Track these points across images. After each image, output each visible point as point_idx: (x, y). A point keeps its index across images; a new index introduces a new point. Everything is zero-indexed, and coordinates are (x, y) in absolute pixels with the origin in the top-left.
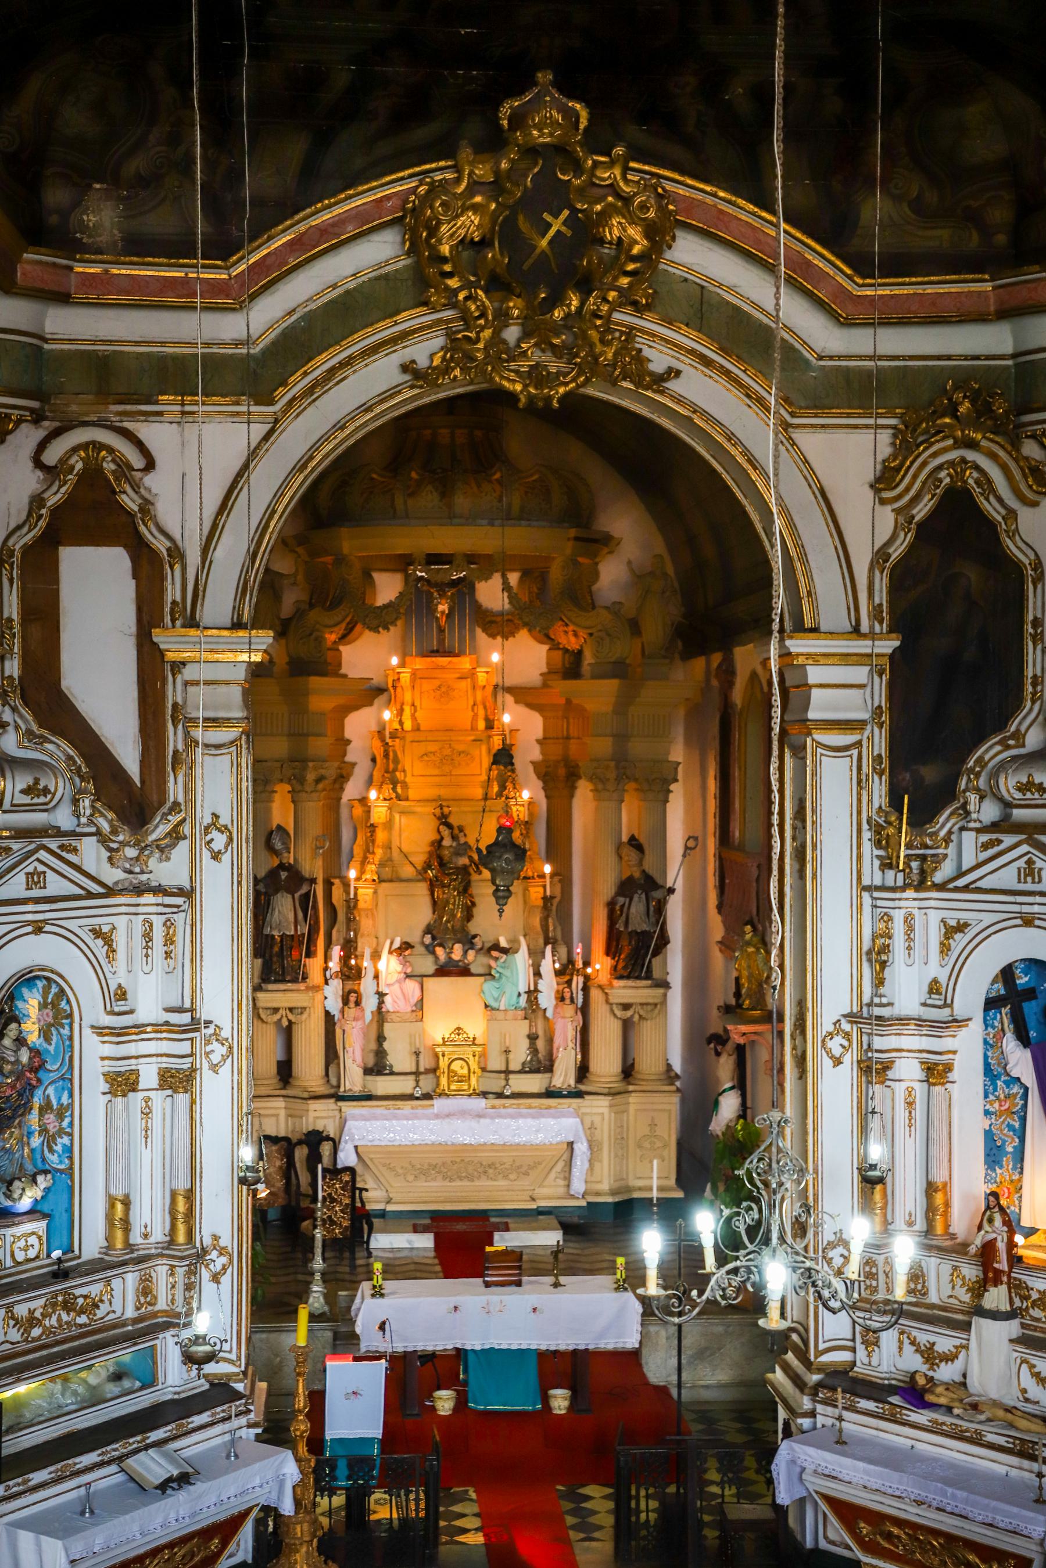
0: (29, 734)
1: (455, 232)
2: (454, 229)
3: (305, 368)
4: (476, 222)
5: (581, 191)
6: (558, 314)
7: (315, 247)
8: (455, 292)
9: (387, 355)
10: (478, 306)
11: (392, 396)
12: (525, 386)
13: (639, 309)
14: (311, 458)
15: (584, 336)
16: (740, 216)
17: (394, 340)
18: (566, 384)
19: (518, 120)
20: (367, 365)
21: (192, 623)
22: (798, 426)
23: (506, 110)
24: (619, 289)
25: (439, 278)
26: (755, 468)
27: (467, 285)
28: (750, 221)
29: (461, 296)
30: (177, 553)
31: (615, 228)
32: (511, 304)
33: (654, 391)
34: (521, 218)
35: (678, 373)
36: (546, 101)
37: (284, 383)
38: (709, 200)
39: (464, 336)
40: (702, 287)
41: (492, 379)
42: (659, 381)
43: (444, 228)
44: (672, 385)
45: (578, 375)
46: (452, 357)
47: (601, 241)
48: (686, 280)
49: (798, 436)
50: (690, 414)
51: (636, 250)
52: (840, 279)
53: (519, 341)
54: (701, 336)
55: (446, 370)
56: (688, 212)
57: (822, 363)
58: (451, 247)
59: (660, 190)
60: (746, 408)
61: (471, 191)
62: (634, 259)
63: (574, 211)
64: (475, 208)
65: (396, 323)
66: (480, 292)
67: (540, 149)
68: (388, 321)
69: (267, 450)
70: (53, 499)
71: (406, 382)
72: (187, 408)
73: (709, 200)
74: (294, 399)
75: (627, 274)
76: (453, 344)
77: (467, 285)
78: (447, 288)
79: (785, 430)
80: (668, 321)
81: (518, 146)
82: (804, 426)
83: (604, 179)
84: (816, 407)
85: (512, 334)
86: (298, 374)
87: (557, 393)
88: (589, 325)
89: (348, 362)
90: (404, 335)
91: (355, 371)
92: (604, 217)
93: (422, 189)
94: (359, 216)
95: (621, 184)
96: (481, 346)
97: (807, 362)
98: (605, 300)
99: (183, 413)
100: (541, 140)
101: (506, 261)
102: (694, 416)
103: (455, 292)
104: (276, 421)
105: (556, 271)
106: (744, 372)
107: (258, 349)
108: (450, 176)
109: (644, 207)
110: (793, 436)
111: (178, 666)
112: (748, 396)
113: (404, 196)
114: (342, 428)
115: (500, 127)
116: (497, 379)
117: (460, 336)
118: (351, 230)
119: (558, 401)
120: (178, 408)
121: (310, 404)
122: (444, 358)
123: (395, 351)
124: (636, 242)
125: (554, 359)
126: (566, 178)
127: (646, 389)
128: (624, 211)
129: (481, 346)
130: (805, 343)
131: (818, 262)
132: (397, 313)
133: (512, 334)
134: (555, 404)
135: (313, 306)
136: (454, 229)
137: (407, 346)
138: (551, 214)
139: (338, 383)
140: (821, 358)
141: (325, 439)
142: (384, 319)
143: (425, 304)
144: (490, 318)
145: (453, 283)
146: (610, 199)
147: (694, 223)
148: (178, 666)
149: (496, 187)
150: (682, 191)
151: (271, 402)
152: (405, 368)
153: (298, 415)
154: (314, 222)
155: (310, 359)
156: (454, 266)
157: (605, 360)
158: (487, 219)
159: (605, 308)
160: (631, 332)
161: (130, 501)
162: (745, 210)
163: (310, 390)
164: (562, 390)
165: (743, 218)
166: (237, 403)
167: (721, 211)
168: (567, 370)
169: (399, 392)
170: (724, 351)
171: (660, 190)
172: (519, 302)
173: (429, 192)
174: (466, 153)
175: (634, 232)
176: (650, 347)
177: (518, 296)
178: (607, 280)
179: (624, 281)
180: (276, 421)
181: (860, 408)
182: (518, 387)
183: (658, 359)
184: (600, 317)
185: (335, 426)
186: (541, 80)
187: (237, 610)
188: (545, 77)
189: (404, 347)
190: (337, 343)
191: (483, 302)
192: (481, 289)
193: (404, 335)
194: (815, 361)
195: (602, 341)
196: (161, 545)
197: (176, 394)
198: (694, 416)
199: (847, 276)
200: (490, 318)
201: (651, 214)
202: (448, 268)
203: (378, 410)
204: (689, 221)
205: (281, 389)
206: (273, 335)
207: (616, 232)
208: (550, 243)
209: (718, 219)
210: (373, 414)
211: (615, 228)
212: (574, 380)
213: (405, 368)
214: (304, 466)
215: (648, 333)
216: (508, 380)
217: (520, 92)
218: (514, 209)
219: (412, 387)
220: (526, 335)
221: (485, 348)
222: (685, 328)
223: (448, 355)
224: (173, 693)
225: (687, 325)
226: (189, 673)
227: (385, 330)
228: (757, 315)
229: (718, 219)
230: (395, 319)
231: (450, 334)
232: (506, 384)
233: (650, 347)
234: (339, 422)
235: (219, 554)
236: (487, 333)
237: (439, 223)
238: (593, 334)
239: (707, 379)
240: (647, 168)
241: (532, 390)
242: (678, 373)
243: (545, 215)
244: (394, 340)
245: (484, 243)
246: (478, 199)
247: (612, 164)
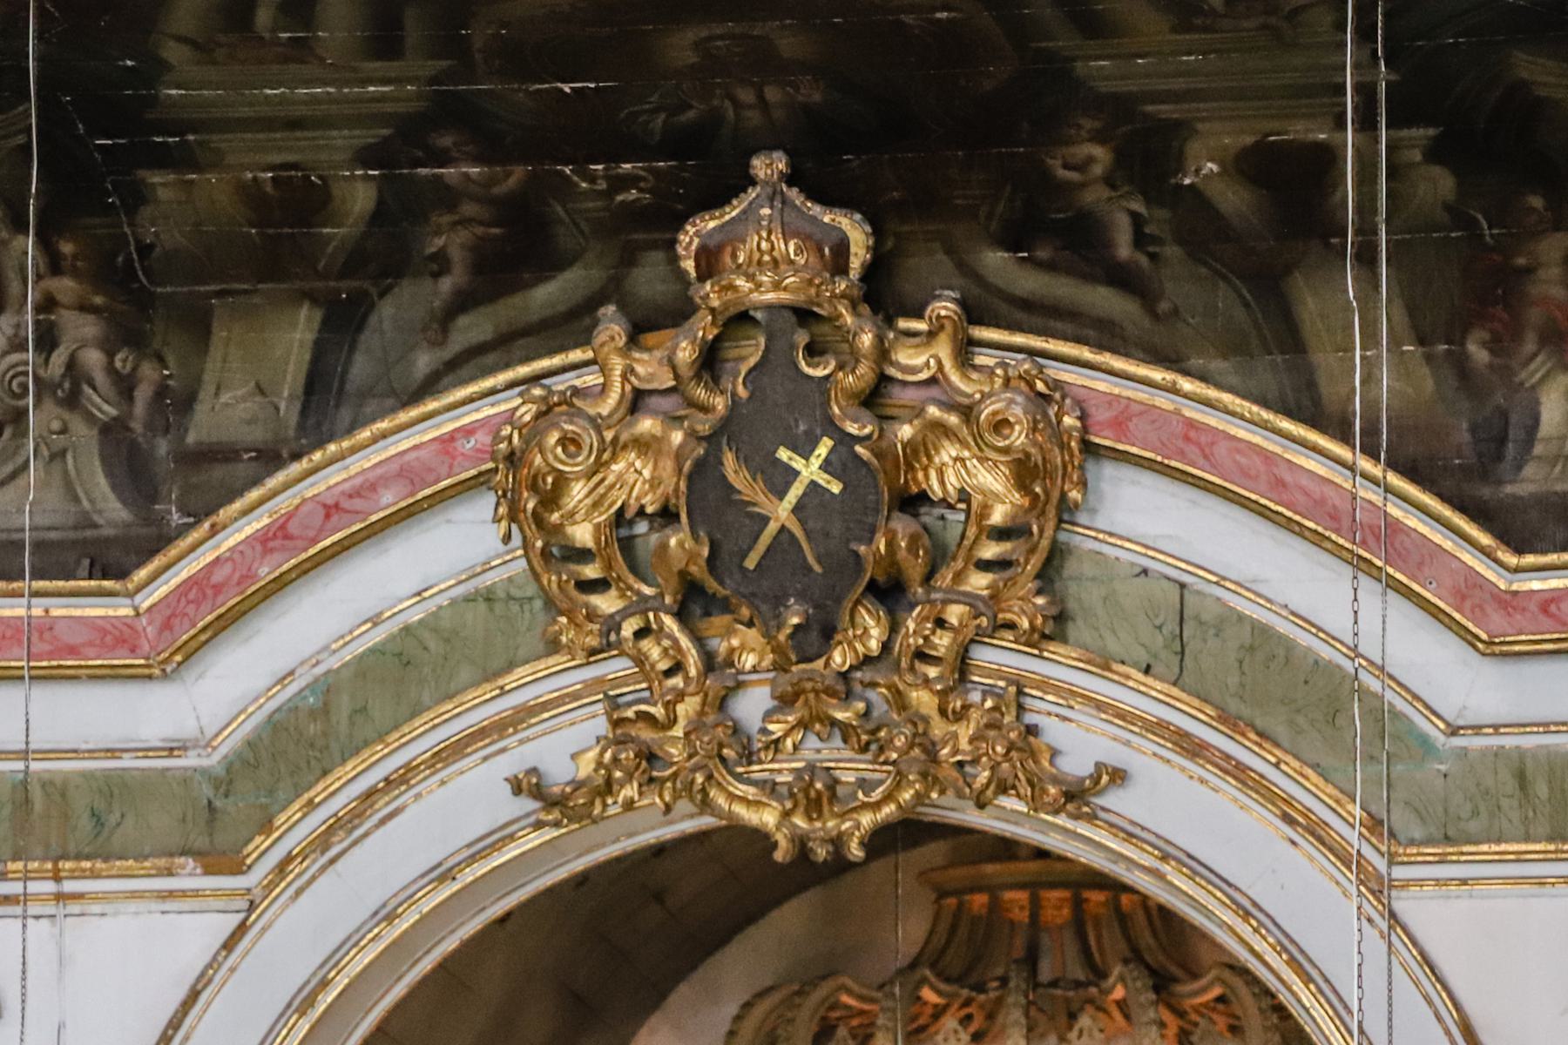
1: (603, 496)
2: (601, 490)
3: (312, 793)
4: (647, 473)
6: (840, 658)
7: (315, 541)
8: (612, 624)
9: (485, 759)
10: (665, 650)
11: (496, 847)
12: (786, 814)
14: (324, 984)
15: (899, 700)
16: (1233, 431)
18: (876, 806)
20: (443, 783)
22: (1407, 884)
23: (690, 237)
24: (969, 599)
25: (574, 593)
26: (1307, 979)
27: (640, 606)
28: (1257, 440)
29: (629, 628)
32: (735, 642)
33: (1076, 817)
34: (729, 459)
35: (1119, 776)
36: (761, 218)
37: (266, 827)
38: (1163, 401)
39: (639, 714)
40: (1183, 586)
41: (706, 805)
42: (1076, 796)
43: (578, 491)
44: (1113, 800)
45: (898, 785)
46: (615, 760)
48: (1145, 572)
49: (1404, 905)
50: (1156, 864)
51: (997, 516)
52: (1469, 558)
53: (768, 716)
54: (1175, 691)
55: (609, 788)
56: (1119, 425)
57: (1457, 742)
58: (597, 527)
59: (1040, 386)
60: (1288, 844)
61: (637, 401)
62: (1001, 534)
63: (845, 441)
64: (643, 445)
65: (503, 692)
66: (669, 622)
67: (759, 315)
68: (487, 686)
69: (232, 970)
71: (528, 815)
72: (69, 886)
73: (1163, 401)
74: (289, 859)
75: (985, 566)
77: (640, 606)
78: (592, 616)
79: (1377, 894)
80: (1103, 663)
81: (713, 311)
82: (1420, 882)
83: (914, 370)
84: (1448, 840)
85: (752, 705)
86: (296, 806)
87: (858, 826)
88: (909, 678)
91: (418, 796)
92: (918, 451)
93: (527, 413)
94: (405, 472)
95: (955, 378)
96: (678, 731)
97: (1425, 741)
98: (940, 623)
99: (60, 897)
100: (755, 296)
101: (706, 552)
102: (1166, 868)
103: (612, 624)
104: (252, 906)
105: (817, 568)
106: (1277, 765)
107: (216, 757)
108: (591, 379)
109: (1001, 425)
110: (1398, 906)
112: (1288, 819)
114: (391, 918)
115: (681, 275)
116: (721, 801)
117: (630, 713)
118: (389, 500)
119: (862, 844)
120: (49, 887)
121: (323, 869)
122: (599, 764)
123: (503, 750)
124: (997, 497)
125: (848, 754)
126: (819, 373)
127: (1056, 812)
128: (964, 432)
129: (678, 731)
130: (1416, 697)
131: (1413, 521)
132: (510, 667)
133: (752, 705)
134: (856, 851)
135: (334, 663)
136: (601, 490)
137: (529, 739)
138: (794, 449)
139: (383, 822)
140: (1454, 731)
141: (352, 942)
142: (476, 684)
143: (553, 646)
144: (693, 672)
145: (607, 603)
146: (933, 411)
147: (1134, 450)
150: (1102, 384)
151: (239, 869)
152: (517, 788)
153: (299, 892)
154: (315, 487)
155: (325, 773)
156: (609, 566)
157: (955, 752)
158: (668, 465)
159: (943, 642)
163: (322, 841)
164: (867, 819)
165: (1242, 434)
166: (170, 873)
167: (1191, 424)
168: (877, 776)
169: (512, 837)
170: (1228, 721)
171: (1040, 386)
172: (753, 636)
173: (539, 416)
176: (1065, 719)
177: (750, 624)
178: (945, 578)
179: (979, 582)
180: (252, 906)
181: (1550, 839)
182: (767, 818)
184: (935, 661)
185: (376, 913)
186: (761, 175)
188: (768, 166)
189: (521, 742)
190: (381, 737)
191: (675, 641)
192: (667, 613)
194: (1442, 738)
195: (943, 712)
197: (44, 859)
198: (1166, 868)
199: (1482, 550)
200: (693, 672)
201: (1018, 438)
202: (591, 571)
203: (469, 875)
204: (1120, 447)
205: (258, 839)
206: (249, 727)
207: (952, 480)
208: (798, 509)
209: (1187, 439)
210: (455, 887)
212: (888, 797)
214: (310, 1001)
215: (1057, 690)
216: (743, 800)
217: (716, 199)
218: (712, 439)
219: (539, 825)
220: (785, 701)
221: (687, 734)
222: (1140, 676)
223: (608, 755)
225: (1147, 671)
227: (480, 707)
228: (1304, 639)
229: (1187, 439)
230: (500, 682)
232: (740, 810)
233: (1065, 719)
234: (384, 905)
236: (687, 709)
237: (562, 480)
238: (923, 700)
239: (1196, 784)
240: (1019, 339)
241: (799, 821)
242: (1119, 776)
243: (783, 454)
245: (667, 515)
246: (647, 425)
247: (931, 335)
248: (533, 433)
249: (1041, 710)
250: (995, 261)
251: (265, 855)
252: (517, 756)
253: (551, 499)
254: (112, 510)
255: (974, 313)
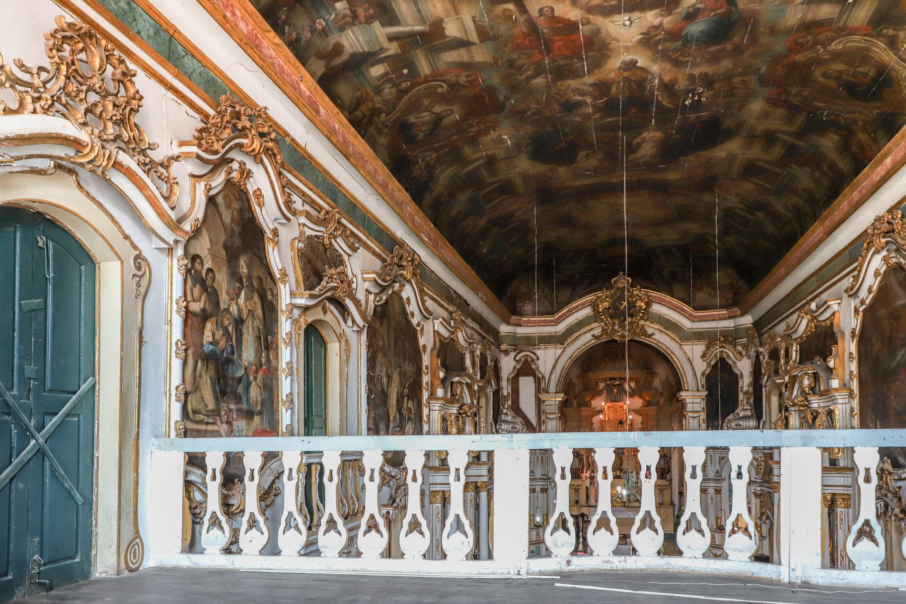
0: (513, 417)
5: (630, 297)
13: (646, 320)
17: (590, 330)
19: (615, 282)
21: (547, 392)
23: (613, 280)
30: (544, 377)
31: (639, 303)
42: (650, 336)
47: (635, 306)
64: (607, 301)
70: (518, 367)
76: (603, 330)
80: (652, 323)
85: (616, 327)
89: (581, 335)
90: (593, 329)
92: (636, 301)
94: (582, 304)
111: (544, 401)
113: (591, 299)
133: (616, 327)
141: (575, 352)
145: (603, 317)
148: (544, 401)
149: (611, 296)
152: (593, 336)
160: (643, 326)
161: (533, 367)
162: (668, 298)
174: (604, 290)
175: (643, 304)
183: (650, 331)
187: (557, 389)
193: (593, 329)
196: (540, 376)
211: (639, 303)
213: (593, 336)
218: (616, 300)
220: (619, 328)
224: (543, 407)
226: (546, 403)
227: (588, 328)
231: (602, 328)
235: (553, 377)
244: (590, 330)
245: (609, 308)
248: (596, 300)
249: (646, 328)
250: (642, 282)
251: (566, 343)
252: (592, 333)
253: (598, 306)
254: (550, 309)
255: (641, 288)
